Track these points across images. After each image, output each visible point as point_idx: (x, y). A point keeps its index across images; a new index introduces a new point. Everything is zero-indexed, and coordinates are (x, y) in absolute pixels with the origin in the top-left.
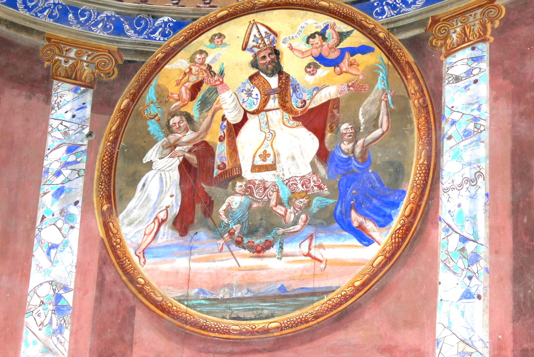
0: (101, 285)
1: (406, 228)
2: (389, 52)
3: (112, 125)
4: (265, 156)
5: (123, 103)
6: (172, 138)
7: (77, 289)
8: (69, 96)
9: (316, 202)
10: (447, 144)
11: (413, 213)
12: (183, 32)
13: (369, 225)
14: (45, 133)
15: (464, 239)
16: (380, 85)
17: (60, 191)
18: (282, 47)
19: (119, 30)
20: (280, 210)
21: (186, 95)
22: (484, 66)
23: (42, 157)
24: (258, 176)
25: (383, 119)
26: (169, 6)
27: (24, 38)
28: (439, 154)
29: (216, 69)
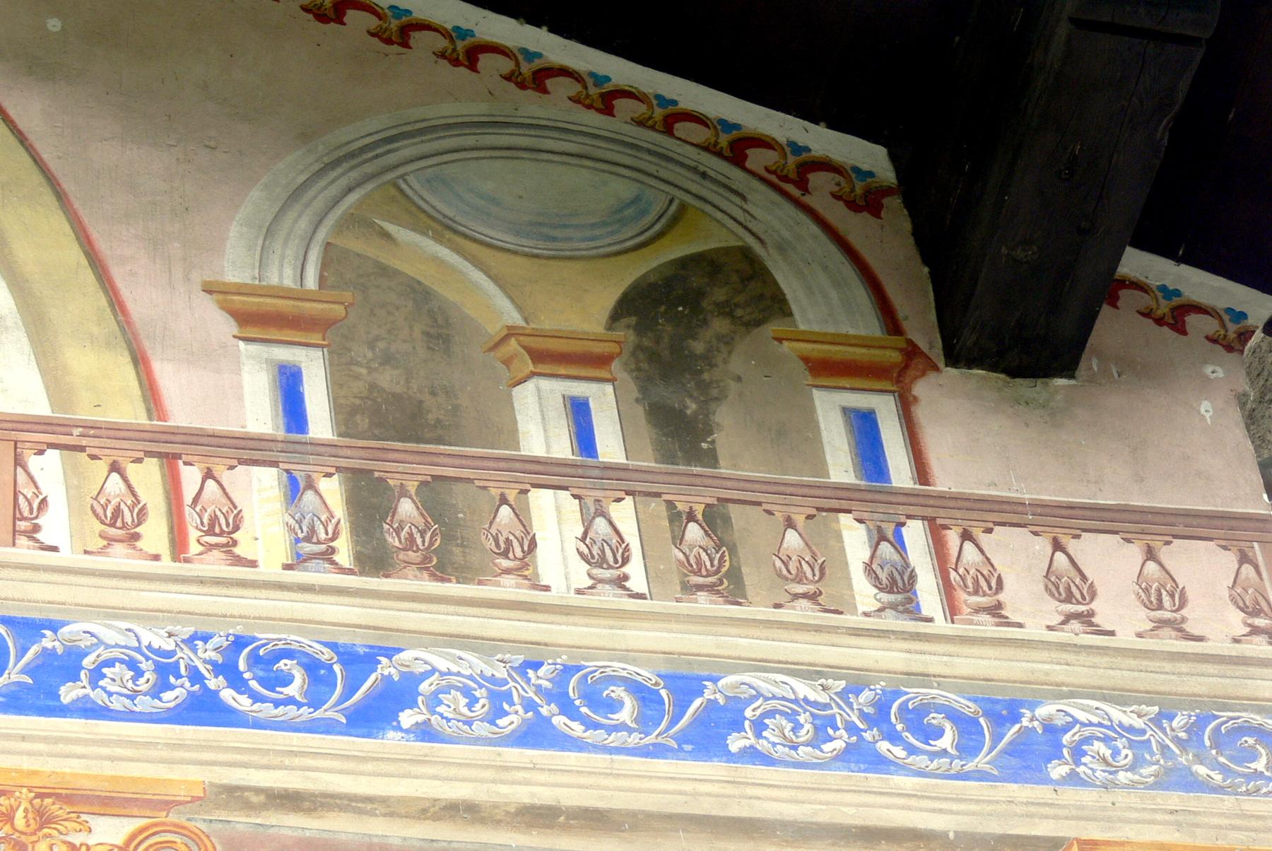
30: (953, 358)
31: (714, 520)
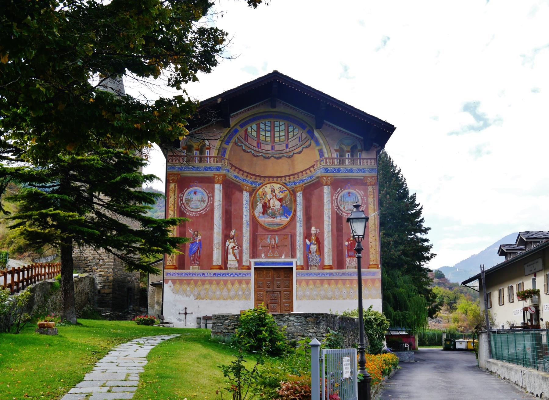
0: (253, 221)
1: (292, 217)
3: (252, 198)
7: (250, 222)
12: (261, 185)
16: (288, 196)
17: (246, 207)
23: (243, 202)
30: (365, 150)
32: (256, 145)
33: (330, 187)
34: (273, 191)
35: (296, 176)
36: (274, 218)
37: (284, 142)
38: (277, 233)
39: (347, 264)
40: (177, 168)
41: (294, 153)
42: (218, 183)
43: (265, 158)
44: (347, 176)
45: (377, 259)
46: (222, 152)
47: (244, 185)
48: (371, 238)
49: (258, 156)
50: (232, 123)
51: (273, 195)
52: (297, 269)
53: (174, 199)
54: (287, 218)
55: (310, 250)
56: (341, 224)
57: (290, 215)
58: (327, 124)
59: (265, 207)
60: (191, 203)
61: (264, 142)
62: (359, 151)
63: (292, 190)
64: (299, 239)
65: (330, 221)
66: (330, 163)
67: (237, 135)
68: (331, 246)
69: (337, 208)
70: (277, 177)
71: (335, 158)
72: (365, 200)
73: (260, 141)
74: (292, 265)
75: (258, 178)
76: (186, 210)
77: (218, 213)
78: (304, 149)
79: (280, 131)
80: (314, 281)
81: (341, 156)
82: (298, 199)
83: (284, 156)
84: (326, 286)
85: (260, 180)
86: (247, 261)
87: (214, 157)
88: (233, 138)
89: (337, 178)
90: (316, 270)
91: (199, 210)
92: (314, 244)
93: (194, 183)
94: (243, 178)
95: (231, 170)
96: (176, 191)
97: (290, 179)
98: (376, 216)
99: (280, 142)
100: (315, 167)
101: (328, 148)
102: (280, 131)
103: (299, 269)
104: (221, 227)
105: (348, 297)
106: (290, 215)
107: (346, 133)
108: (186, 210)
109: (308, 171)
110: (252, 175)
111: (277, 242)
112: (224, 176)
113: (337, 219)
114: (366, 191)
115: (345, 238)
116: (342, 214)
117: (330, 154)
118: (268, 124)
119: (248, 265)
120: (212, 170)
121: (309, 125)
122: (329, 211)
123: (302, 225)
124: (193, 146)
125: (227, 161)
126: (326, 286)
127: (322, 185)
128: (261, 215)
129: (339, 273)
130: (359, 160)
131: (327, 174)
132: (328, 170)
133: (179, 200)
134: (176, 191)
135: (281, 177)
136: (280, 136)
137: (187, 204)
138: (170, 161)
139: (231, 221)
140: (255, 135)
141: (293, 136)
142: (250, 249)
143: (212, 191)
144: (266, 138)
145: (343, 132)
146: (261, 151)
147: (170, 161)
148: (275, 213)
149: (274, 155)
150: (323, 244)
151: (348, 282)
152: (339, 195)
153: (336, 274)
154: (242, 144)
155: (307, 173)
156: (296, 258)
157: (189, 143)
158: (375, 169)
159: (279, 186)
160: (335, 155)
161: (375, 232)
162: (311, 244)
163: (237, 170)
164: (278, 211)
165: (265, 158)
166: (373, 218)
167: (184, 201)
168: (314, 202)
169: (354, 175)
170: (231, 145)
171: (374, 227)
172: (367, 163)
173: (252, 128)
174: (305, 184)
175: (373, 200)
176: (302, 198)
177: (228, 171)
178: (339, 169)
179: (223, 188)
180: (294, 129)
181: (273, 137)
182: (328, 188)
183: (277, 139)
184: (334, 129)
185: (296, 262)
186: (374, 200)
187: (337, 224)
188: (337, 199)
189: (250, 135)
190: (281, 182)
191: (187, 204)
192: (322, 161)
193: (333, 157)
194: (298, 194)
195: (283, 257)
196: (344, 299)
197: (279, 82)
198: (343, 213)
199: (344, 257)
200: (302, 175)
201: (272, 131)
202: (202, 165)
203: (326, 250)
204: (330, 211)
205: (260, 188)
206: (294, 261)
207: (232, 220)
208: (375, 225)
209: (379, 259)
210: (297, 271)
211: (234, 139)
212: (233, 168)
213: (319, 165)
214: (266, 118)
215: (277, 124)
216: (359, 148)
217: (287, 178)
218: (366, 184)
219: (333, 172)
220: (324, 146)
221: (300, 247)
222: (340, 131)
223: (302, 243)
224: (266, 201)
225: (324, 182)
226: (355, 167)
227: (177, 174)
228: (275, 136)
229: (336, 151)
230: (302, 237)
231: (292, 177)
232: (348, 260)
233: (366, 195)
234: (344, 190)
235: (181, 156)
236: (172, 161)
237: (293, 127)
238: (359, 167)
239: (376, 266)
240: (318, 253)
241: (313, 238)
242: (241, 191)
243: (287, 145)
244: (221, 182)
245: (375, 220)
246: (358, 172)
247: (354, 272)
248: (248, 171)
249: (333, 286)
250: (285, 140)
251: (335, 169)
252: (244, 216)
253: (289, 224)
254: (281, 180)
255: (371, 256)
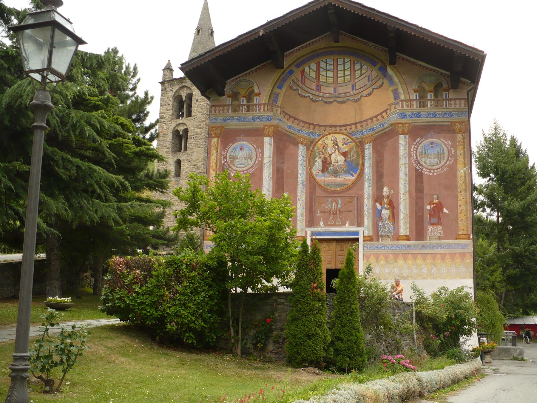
0: (310, 181)
1: (359, 175)
2: (356, 143)
4: (336, 160)
5: (311, 149)
6: (320, 156)
8: (302, 147)
9: (345, 169)
10: (366, 160)
11: (360, 172)
12: (321, 136)
13: (353, 173)
14: (298, 154)
15: (368, 177)
16: (354, 149)
17: (301, 164)
18: (338, 141)
19: (309, 135)
20: (339, 170)
21: (322, 148)
22: (371, 147)
24: (335, 164)
25: (355, 155)
26: (318, 131)
27: (292, 135)
28: (364, 162)
29: (327, 144)
31: (437, 102)
32: (314, 87)
33: (407, 136)
34: (335, 143)
35: (364, 124)
36: (336, 177)
37: (350, 83)
38: (341, 195)
39: (429, 234)
40: (221, 119)
41: (361, 96)
42: (268, 135)
43: (326, 102)
44: (430, 122)
45: (467, 227)
46: (273, 97)
47: (299, 137)
48: (460, 200)
49: (317, 101)
50: (286, 63)
51: (335, 148)
52: (364, 241)
53: (217, 157)
54: (353, 176)
55: (381, 217)
56: (422, 182)
57: (356, 173)
58: (403, 59)
59: (326, 164)
60: (236, 161)
61: (325, 84)
62: (445, 90)
63: (359, 142)
64: (368, 203)
65: (408, 179)
66: (407, 106)
67: (293, 77)
68: (408, 210)
69: (417, 162)
70: (341, 126)
71: (414, 100)
72: (453, 151)
73: (321, 83)
74: (359, 236)
75: (317, 128)
76: (230, 169)
77: (268, 172)
78: (374, 90)
79: (344, 70)
80: (386, 256)
81: (421, 97)
82: (367, 152)
83: (349, 100)
84: (401, 262)
85: (319, 130)
86: (302, 230)
87: (264, 105)
88: (287, 82)
89: (416, 125)
90: (389, 242)
91: (245, 169)
92: (386, 209)
93: (240, 136)
94: (299, 128)
95: (285, 120)
96: (219, 147)
97: (356, 128)
98: (467, 172)
99: (344, 82)
100: (388, 111)
101: (405, 87)
102: (344, 70)
103: (367, 240)
104: (271, 190)
105: (430, 277)
106: (356, 173)
107: (427, 68)
108: (230, 169)
109: (379, 117)
110: (310, 124)
111: (339, 206)
112: (276, 127)
113: (416, 177)
114: (453, 140)
115: (426, 200)
116: (422, 170)
117: (407, 96)
118: (330, 61)
119: (304, 235)
120: (261, 121)
121: (381, 61)
122: (405, 167)
123: (371, 185)
124: (239, 93)
125: (279, 109)
126: (401, 262)
127: (398, 134)
128: (320, 173)
129: (418, 246)
130: (444, 102)
131: (404, 120)
132: (405, 115)
133: (222, 158)
134: (219, 147)
135: (346, 126)
136: (344, 76)
137: (232, 162)
138: (213, 112)
139: (283, 182)
140: (314, 76)
141: (361, 75)
142: (306, 215)
143: (261, 146)
144: (328, 79)
145: (424, 67)
146: (321, 94)
147: (213, 112)
148: (337, 170)
149: (338, 100)
150: (398, 208)
151: (429, 257)
152: (418, 146)
153: (414, 246)
154: (298, 88)
155: (378, 120)
156: (363, 226)
157: (235, 90)
158: (466, 112)
159: (343, 136)
160: (414, 96)
161: (466, 192)
162: (382, 208)
163: (291, 119)
164: (341, 167)
165: (326, 102)
166: (463, 175)
167: (228, 158)
168: (387, 156)
169: (439, 120)
170: (284, 89)
171: (464, 186)
172: (455, 104)
173: (310, 68)
174: (376, 133)
175: (463, 151)
176: (371, 151)
177: (281, 120)
178: (419, 113)
179: (274, 141)
180: (361, 67)
181: (336, 77)
182: (405, 137)
183: (340, 80)
184: (413, 64)
185: (363, 232)
186: (464, 152)
187: (416, 183)
188: (416, 151)
189: (307, 76)
190: (345, 132)
191: (232, 162)
192: (397, 104)
193: (411, 99)
194: (367, 146)
195: (347, 225)
196: (424, 278)
197: (335, 5)
198: (424, 169)
199: (425, 225)
200: (372, 123)
201: (335, 71)
202: (250, 115)
203: (402, 216)
204: (408, 166)
205: (319, 140)
206: (361, 230)
207: (285, 180)
208: (466, 183)
209: (470, 227)
210: (365, 242)
211: (289, 82)
212: (287, 117)
213: (393, 110)
214: (327, 55)
215: (340, 61)
216: (445, 86)
217: (353, 127)
218: (454, 131)
219: (411, 117)
220: (400, 86)
221: (368, 212)
222: (420, 66)
223: (371, 207)
224: (327, 156)
225: (400, 130)
226: (439, 110)
227: (220, 127)
228: (339, 76)
229: (415, 91)
230: (371, 201)
231: (358, 125)
232: (430, 228)
233: (454, 146)
234: (426, 139)
235: (224, 106)
236: (215, 112)
237: (361, 64)
238: (445, 110)
239: (467, 237)
240: (391, 219)
241: (385, 201)
242: (296, 144)
243: (353, 86)
244: (271, 134)
245: (465, 177)
246: (443, 117)
247: (437, 244)
248: (304, 120)
249: (410, 262)
250: (351, 81)
251: (414, 114)
252: (299, 175)
253: (355, 183)
254: (346, 130)
255: (460, 223)
